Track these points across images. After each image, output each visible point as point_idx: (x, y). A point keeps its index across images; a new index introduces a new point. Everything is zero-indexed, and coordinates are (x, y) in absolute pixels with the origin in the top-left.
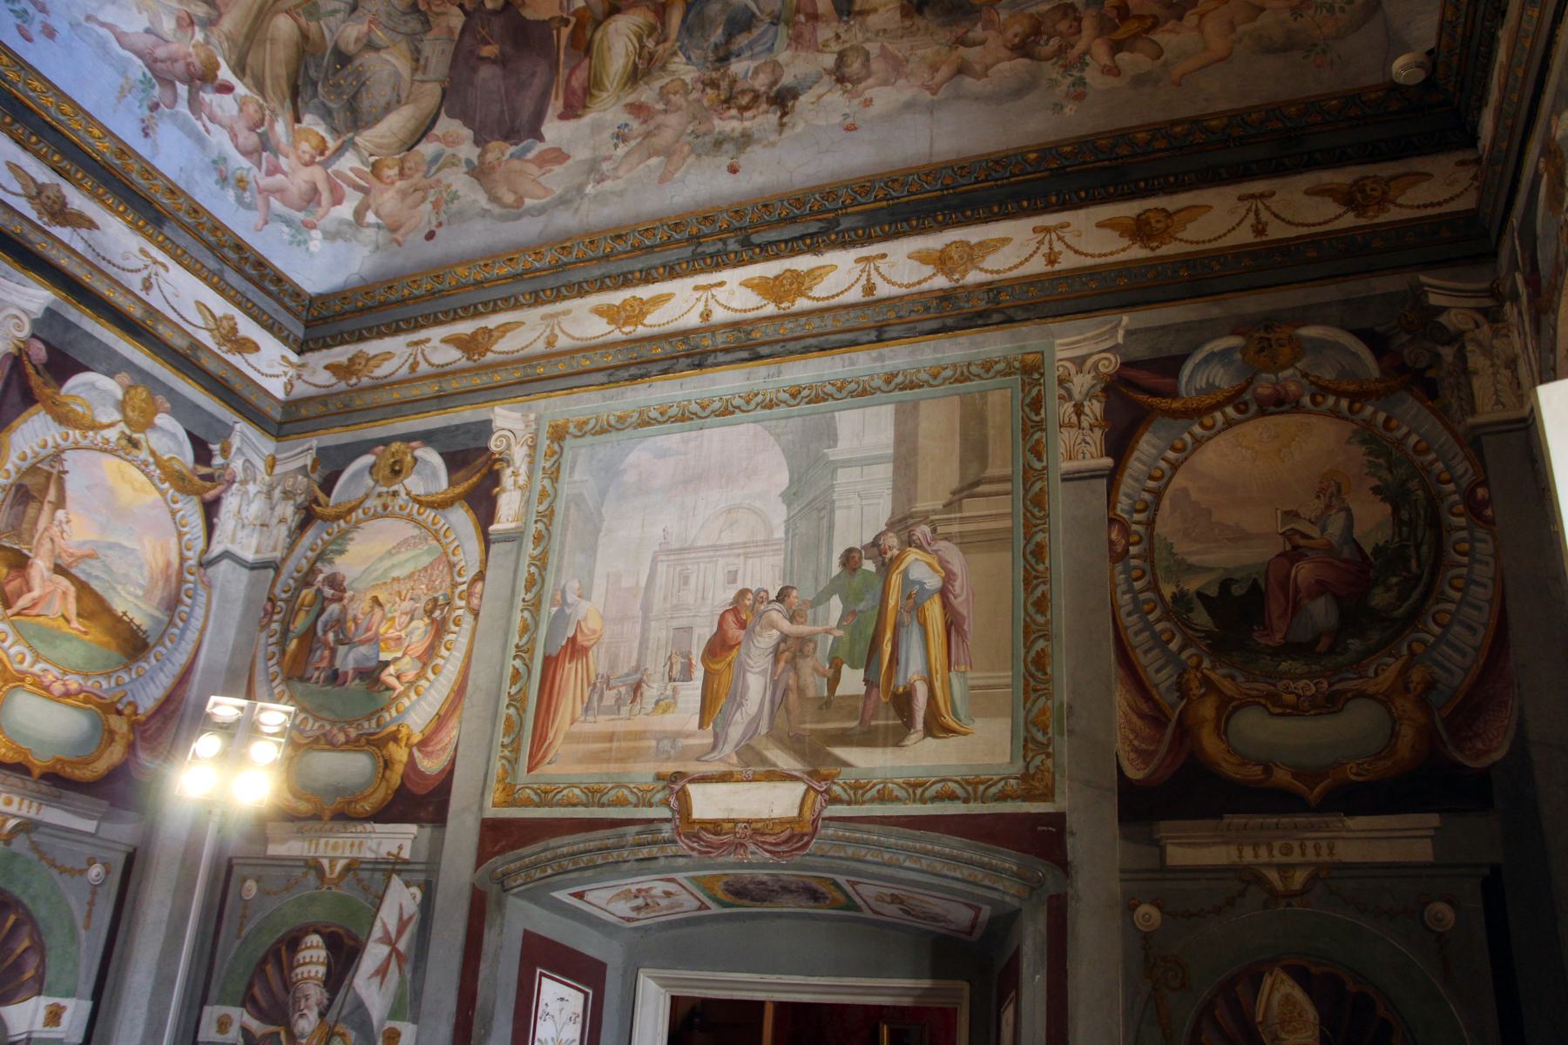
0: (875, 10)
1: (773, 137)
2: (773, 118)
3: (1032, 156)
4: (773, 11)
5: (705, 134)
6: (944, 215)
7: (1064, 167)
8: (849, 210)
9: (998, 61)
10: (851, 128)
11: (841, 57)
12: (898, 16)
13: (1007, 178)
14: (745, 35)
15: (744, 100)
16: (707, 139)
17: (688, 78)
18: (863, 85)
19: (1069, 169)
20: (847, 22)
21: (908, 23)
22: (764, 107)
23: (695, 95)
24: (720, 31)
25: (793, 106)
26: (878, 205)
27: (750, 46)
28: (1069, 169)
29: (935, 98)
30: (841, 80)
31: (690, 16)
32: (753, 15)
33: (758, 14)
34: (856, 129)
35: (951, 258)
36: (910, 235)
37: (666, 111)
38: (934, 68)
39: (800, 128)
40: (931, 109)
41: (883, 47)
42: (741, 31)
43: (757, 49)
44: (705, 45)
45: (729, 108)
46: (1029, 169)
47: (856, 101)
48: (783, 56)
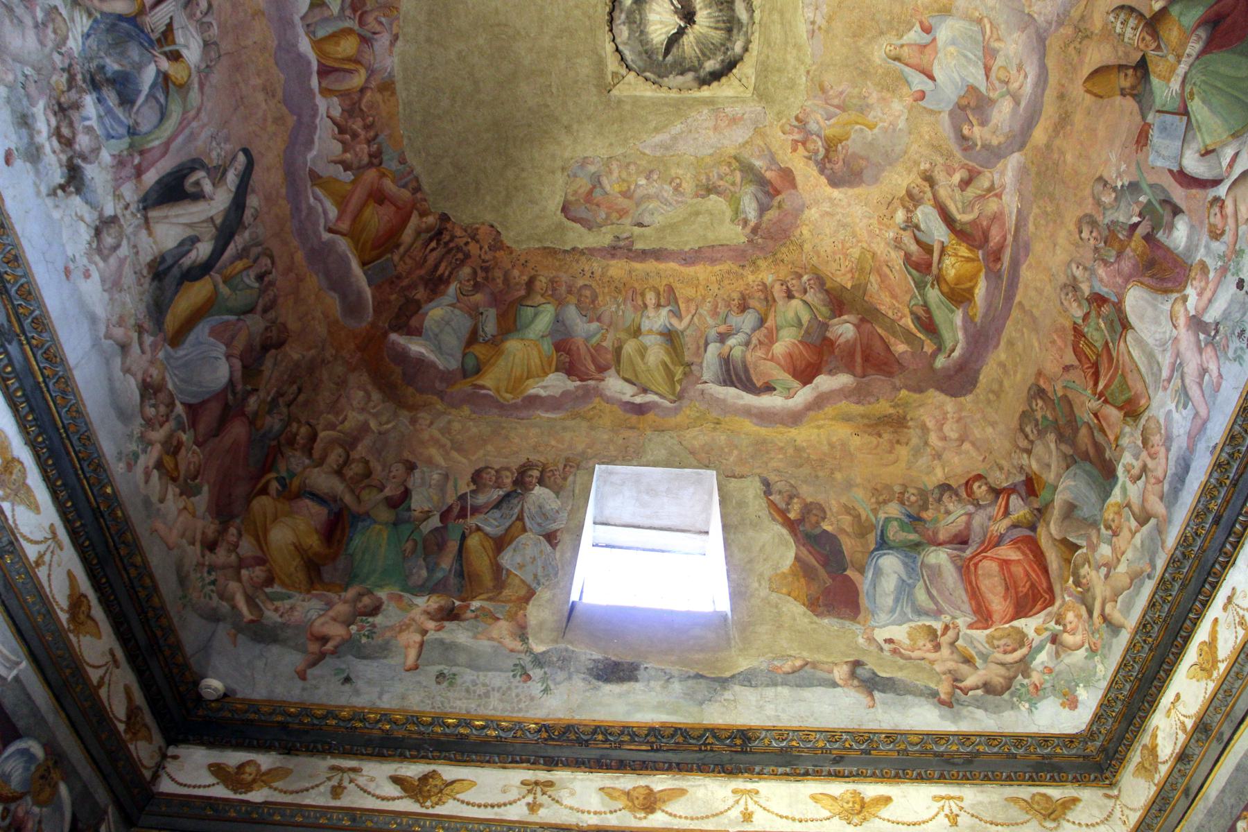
0: (150, 234)
1: (44, 190)
2: (58, 177)
3: (109, 490)
4: (137, 124)
5: (28, 96)
6: (43, 442)
7: (102, 516)
8: (27, 348)
9: (134, 375)
10: (67, 272)
11: (114, 220)
12: (149, 259)
13: (85, 476)
14: (117, 102)
15: (65, 131)
16: (25, 102)
17: (71, 43)
18: (97, 258)
19: (102, 520)
20: (138, 210)
21: (145, 272)
22: (64, 158)
23: (57, 58)
24: (116, 67)
25: (72, 193)
26: (39, 373)
27: (109, 111)
28: (102, 520)
29: (103, 340)
30: (98, 232)
31: (125, 25)
32: (133, 103)
33: (135, 108)
34: (67, 277)
35: (11, 473)
36: (15, 416)
37: (36, 26)
38: (121, 322)
39: (57, 215)
40: (96, 344)
41: (126, 258)
42: (119, 94)
43: (107, 121)
44: (102, 54)
45: (55, 114)
46: (95, 490)
47: (85, 261)
48: (106, 156)
